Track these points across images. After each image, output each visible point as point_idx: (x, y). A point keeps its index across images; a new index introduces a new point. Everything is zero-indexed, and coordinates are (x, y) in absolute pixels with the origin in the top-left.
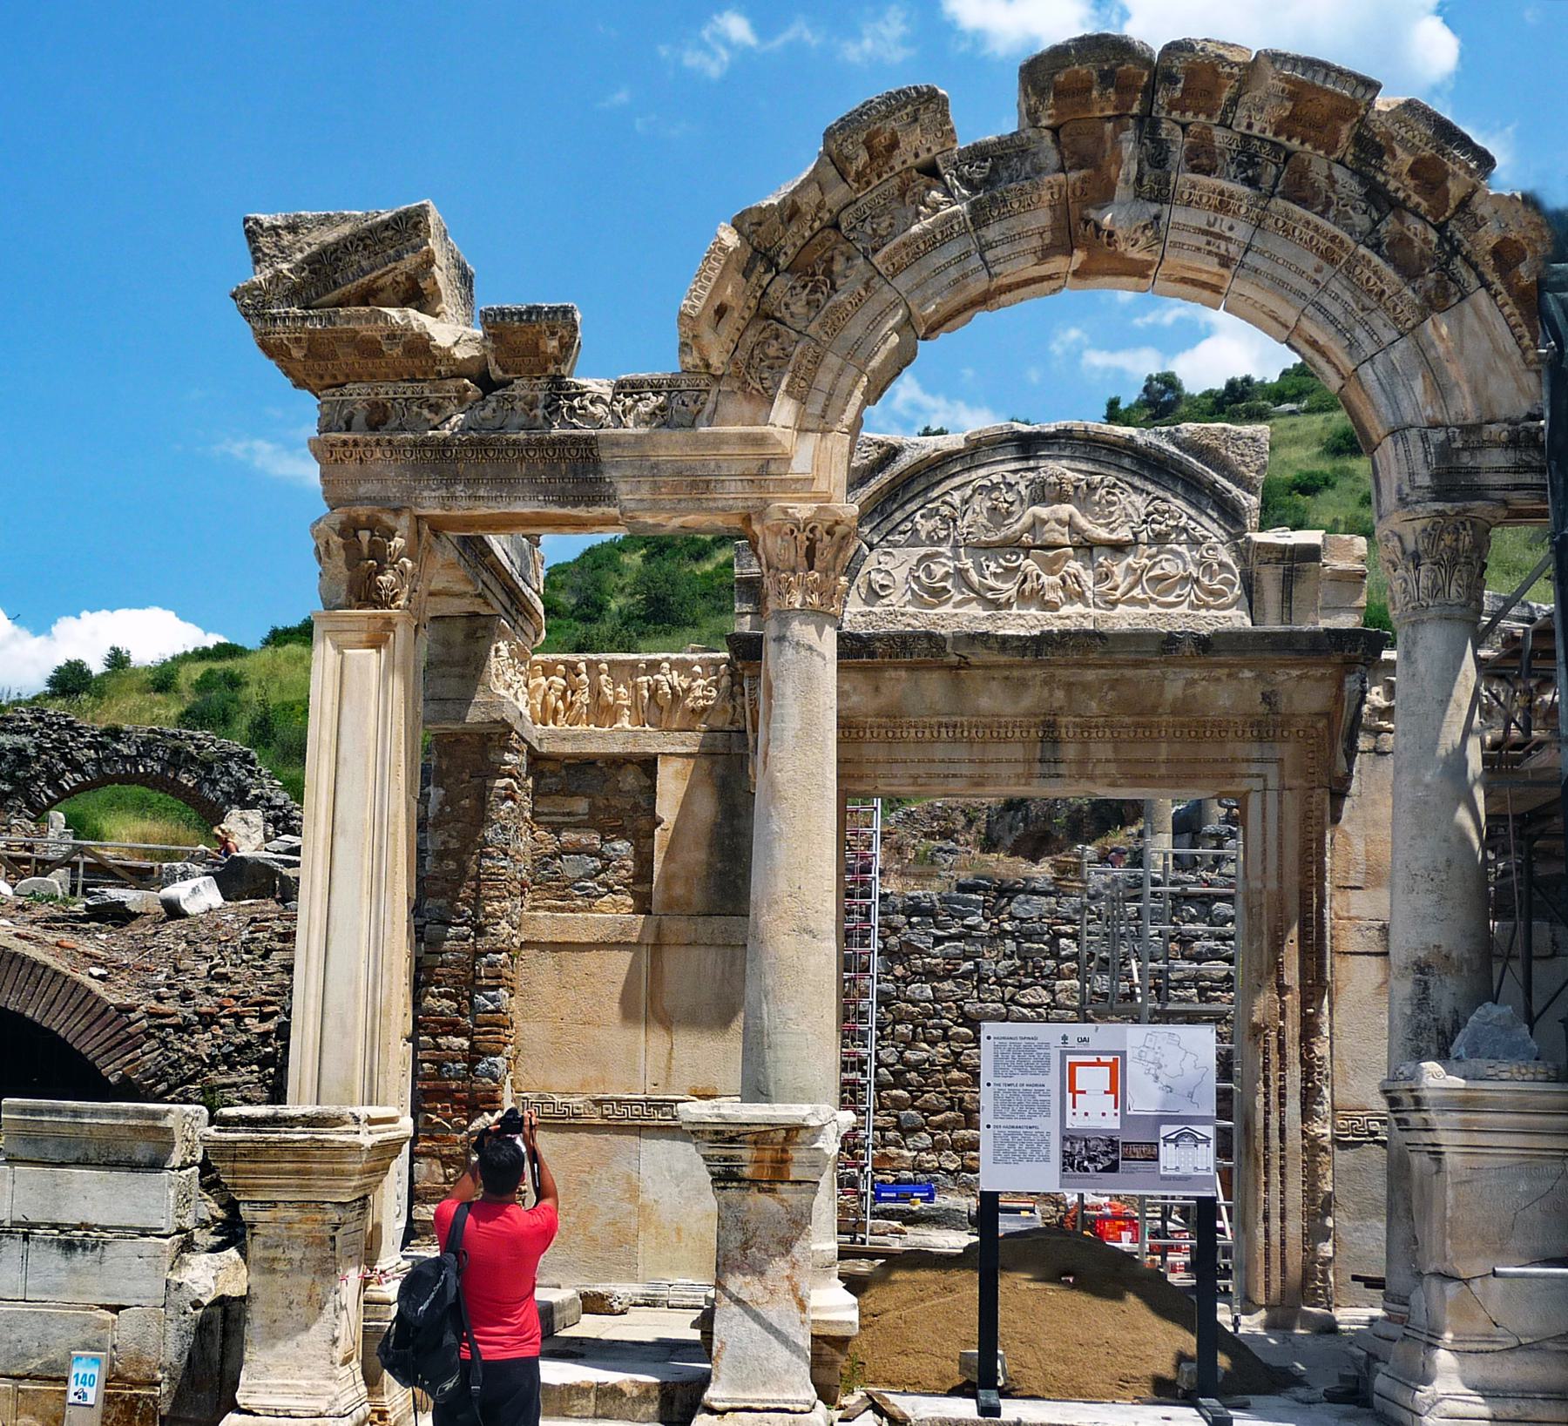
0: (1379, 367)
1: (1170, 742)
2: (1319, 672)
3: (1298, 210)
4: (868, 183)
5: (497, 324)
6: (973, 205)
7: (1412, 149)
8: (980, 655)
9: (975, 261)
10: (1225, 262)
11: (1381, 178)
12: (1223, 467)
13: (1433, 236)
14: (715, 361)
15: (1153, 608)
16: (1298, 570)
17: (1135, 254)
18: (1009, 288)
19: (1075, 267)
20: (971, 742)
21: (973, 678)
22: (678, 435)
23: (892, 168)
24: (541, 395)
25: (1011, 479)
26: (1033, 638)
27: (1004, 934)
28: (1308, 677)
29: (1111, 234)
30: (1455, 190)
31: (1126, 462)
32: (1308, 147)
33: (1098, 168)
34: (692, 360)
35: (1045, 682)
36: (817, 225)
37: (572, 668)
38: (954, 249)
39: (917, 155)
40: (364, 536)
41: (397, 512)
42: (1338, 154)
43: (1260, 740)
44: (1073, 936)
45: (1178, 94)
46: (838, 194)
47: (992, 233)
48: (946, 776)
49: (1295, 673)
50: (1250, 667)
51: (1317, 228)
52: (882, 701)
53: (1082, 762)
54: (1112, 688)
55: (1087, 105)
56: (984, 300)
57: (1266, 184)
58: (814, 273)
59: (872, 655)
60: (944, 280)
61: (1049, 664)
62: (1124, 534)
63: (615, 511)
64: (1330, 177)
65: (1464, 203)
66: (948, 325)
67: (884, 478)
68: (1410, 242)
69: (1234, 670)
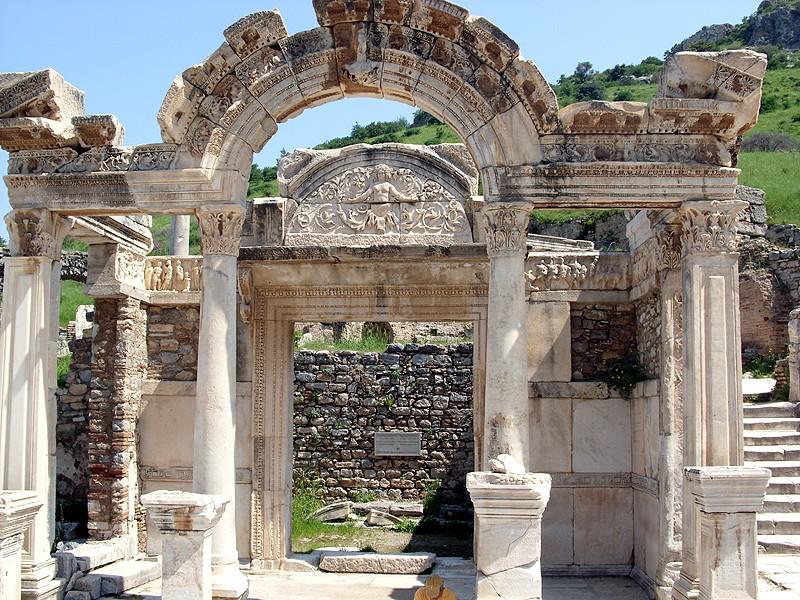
0: (476, 138)
1: (436, 297)
3: (438, 66)
4: (247, 54)
5: (80, 125)
6: (293, 64)
7: (484, 39)
8: (343, 257)
9: (296, 89)
10: (408, 88)
11: (474, 51)
12: (460, 165)
13: (499, 78)
14: (177, 138)
15: (426, 233)
17: (366, 84)
18: (315, 99)
19: (344, 89)
20: (345, 297)
21: (342, 268)
22: (160, 173)
24: (103, 154)
25: (363, 170)
27: (409, 373)
29: (354, 77)
30: (505, 60)
31: (416, 162)
32: (442, 36)
33: (349, 46)
34: (167, 138)
35: (375, 269)
36: (224, 73)
37: (165, 262)
38: (286, 83)
40: (26, 222)
41: (40, 210)
42: (456, 40)
43: (478, 296)
44: (441, 374)
45: (383, 13)
46: (233, 60)
47: (302, 76)
50: (469, 262)
51: (446, 74)
52: (302, 278)
53: (396, 307)
55: (344, 17)
56: (305, 104)
57: (425, 53)
58: (223, 96)
59: (294, 257)
60: (282, 98)
62: (414, 197)
63: (135, 208)
65: (510, 64)
67: (305, 170)
68: (489, 80)
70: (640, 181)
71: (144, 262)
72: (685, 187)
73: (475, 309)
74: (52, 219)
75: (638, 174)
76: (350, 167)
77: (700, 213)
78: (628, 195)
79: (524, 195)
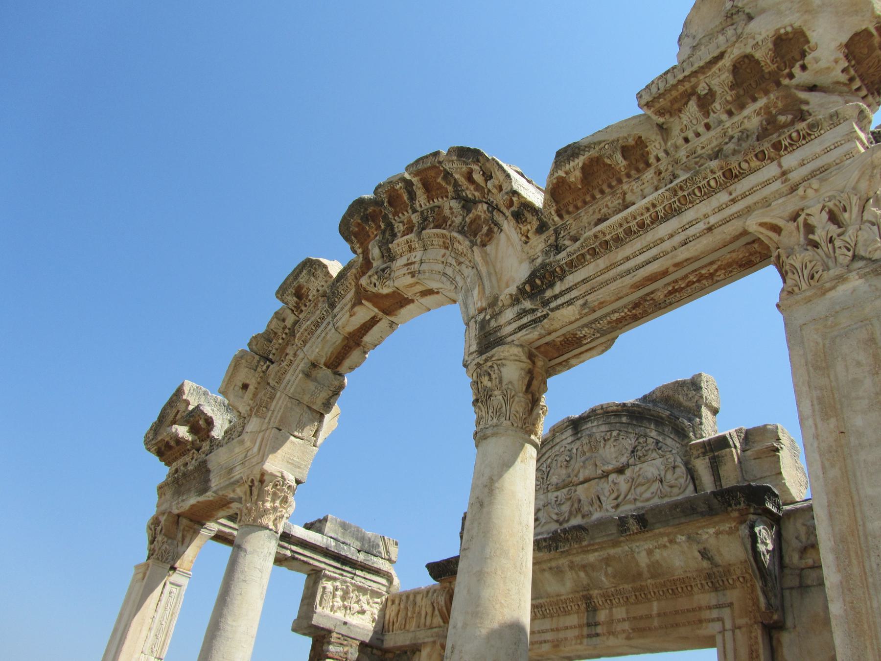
1: (658, 600)
2: (726, 527)
4: (302, 311)
16: (718, 456)
20: (552, 617)
23: (310, 301)
25: (568, 447)
26: (550, 538)
28: (721, 533)
39: (318, 291)
43: (716, 590)
47: (336, 310)
48: (541, 643)
49: (712, 531)
54: (608, 565)
60: (319, 340)
61: (567, 553)
64: (451, 208)
66: (347, 363)
69: (671, 537)
70: (663, 230)
71: (384, 599)
72: (744, 196)
73: (715, 614)
74: (178, 523)
75: (657, 220)
76: (557, 448)
77: (781, 223)
78: (648, 262)
79: (506, 337)
